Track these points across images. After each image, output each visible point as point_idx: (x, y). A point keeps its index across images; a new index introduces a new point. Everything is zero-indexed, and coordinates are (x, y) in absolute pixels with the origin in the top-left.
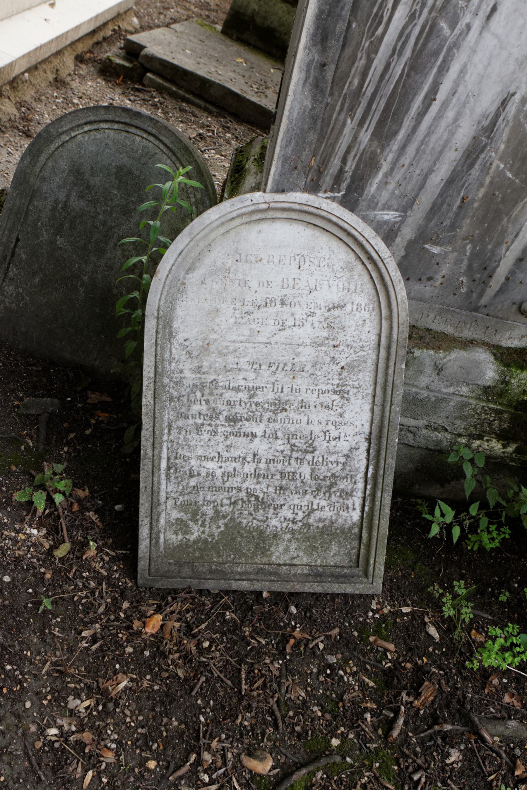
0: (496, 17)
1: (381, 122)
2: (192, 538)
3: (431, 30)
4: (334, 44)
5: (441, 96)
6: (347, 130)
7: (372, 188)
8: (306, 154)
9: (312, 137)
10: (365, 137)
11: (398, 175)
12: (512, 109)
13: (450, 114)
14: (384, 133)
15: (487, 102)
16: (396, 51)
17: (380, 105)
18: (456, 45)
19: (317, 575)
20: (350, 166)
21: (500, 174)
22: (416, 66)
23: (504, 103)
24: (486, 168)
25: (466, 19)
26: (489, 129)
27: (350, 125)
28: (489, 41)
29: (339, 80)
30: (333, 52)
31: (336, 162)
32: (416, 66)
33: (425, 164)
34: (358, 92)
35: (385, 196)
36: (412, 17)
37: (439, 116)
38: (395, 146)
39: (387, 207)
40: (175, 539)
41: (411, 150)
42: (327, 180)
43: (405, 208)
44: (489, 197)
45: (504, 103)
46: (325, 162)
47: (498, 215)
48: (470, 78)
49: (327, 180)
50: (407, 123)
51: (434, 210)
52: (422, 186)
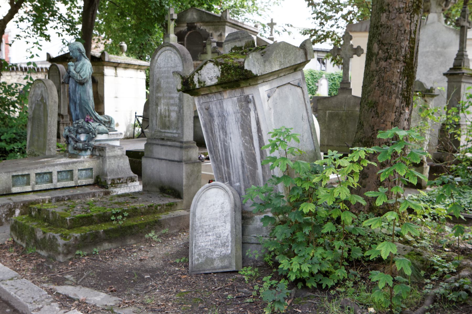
0: (232, 139)
1: (227, 165)
2: (200, 262)
3: (224, 145)
4: (213, 152)
5: (232, 156)
6: (223, 168)
7: (232, 179)
8: (219, 175)
9: (218, 171)
10: (226, 168)
11: (234, 174)
12: (243, 154)
13: (235, 159)
14: (228, 167)
15: (239, 155)
16: (222, 151)
17: (225, 161)
18: (229, 146)
19: (222, 268)
20: (227, 175)
21: (249, 168)
22: (226, 152)
23: (242, 154)
24: (246, 167)
25: (228, 142)
26: (242, 160)
27: (223, 167)
28: (233, 144)
29: (217, 159)
30: (214, 154)
31: (224, 175)
32: (226, 152)
33: (237, 171)
34: (221, 160)
35: (235, 180)
36: (221, 144)
37: (234, 160)
38: (231, 169)
39: (237, 182)
40: (196, 263)
41: (234, 169)
42: (225, 180)
43: (239, 181)
44: (251, 174)
45: (242, 154)
46: (223, 176)
47: (254, 177)
48: (234, 151)
49: (225, 180)
50: (230, 163)
51: (244, 180)
52: (239, 176)
